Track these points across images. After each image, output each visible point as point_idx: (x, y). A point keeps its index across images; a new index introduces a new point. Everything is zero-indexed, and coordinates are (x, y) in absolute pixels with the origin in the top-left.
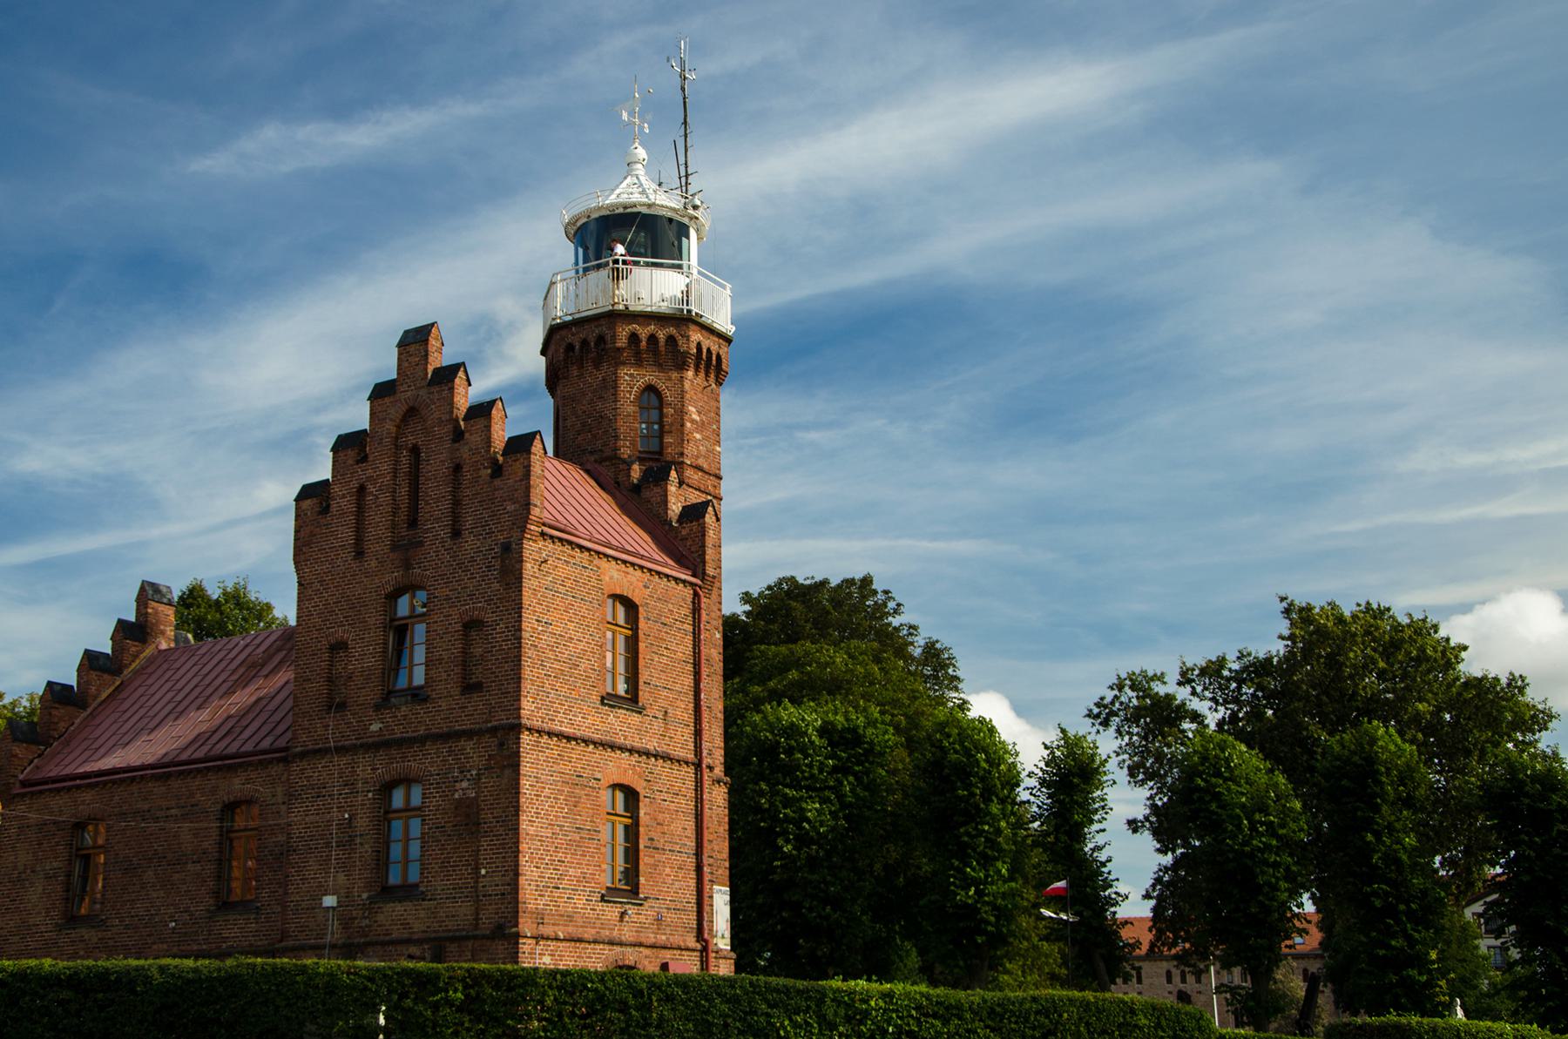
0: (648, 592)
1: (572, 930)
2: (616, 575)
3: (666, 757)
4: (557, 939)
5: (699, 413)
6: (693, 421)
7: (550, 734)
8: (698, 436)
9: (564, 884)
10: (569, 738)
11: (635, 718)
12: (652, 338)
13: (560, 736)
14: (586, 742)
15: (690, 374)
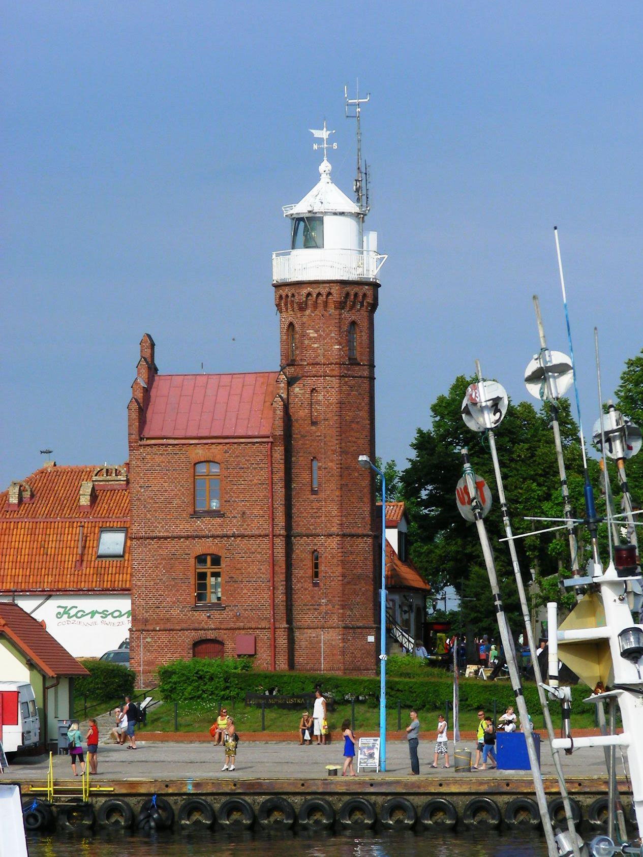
0: (227, 455)
1: (168, 626)
2: (200, 452)
3: (243, 536)
4: (154, 630)
5: (316, 331)
6: (311, 338)
7: (152, 538)
8: (316, 345)
9: (164, 604)
10: (166, 538)
11: (219, 520)
12: (287, 296)
13: (159, 538)
14: (179, 538)
15: (308, 312)
